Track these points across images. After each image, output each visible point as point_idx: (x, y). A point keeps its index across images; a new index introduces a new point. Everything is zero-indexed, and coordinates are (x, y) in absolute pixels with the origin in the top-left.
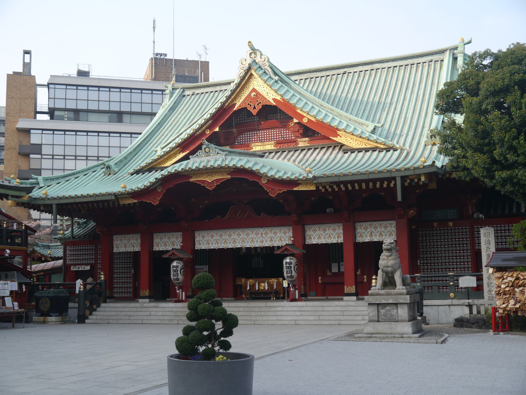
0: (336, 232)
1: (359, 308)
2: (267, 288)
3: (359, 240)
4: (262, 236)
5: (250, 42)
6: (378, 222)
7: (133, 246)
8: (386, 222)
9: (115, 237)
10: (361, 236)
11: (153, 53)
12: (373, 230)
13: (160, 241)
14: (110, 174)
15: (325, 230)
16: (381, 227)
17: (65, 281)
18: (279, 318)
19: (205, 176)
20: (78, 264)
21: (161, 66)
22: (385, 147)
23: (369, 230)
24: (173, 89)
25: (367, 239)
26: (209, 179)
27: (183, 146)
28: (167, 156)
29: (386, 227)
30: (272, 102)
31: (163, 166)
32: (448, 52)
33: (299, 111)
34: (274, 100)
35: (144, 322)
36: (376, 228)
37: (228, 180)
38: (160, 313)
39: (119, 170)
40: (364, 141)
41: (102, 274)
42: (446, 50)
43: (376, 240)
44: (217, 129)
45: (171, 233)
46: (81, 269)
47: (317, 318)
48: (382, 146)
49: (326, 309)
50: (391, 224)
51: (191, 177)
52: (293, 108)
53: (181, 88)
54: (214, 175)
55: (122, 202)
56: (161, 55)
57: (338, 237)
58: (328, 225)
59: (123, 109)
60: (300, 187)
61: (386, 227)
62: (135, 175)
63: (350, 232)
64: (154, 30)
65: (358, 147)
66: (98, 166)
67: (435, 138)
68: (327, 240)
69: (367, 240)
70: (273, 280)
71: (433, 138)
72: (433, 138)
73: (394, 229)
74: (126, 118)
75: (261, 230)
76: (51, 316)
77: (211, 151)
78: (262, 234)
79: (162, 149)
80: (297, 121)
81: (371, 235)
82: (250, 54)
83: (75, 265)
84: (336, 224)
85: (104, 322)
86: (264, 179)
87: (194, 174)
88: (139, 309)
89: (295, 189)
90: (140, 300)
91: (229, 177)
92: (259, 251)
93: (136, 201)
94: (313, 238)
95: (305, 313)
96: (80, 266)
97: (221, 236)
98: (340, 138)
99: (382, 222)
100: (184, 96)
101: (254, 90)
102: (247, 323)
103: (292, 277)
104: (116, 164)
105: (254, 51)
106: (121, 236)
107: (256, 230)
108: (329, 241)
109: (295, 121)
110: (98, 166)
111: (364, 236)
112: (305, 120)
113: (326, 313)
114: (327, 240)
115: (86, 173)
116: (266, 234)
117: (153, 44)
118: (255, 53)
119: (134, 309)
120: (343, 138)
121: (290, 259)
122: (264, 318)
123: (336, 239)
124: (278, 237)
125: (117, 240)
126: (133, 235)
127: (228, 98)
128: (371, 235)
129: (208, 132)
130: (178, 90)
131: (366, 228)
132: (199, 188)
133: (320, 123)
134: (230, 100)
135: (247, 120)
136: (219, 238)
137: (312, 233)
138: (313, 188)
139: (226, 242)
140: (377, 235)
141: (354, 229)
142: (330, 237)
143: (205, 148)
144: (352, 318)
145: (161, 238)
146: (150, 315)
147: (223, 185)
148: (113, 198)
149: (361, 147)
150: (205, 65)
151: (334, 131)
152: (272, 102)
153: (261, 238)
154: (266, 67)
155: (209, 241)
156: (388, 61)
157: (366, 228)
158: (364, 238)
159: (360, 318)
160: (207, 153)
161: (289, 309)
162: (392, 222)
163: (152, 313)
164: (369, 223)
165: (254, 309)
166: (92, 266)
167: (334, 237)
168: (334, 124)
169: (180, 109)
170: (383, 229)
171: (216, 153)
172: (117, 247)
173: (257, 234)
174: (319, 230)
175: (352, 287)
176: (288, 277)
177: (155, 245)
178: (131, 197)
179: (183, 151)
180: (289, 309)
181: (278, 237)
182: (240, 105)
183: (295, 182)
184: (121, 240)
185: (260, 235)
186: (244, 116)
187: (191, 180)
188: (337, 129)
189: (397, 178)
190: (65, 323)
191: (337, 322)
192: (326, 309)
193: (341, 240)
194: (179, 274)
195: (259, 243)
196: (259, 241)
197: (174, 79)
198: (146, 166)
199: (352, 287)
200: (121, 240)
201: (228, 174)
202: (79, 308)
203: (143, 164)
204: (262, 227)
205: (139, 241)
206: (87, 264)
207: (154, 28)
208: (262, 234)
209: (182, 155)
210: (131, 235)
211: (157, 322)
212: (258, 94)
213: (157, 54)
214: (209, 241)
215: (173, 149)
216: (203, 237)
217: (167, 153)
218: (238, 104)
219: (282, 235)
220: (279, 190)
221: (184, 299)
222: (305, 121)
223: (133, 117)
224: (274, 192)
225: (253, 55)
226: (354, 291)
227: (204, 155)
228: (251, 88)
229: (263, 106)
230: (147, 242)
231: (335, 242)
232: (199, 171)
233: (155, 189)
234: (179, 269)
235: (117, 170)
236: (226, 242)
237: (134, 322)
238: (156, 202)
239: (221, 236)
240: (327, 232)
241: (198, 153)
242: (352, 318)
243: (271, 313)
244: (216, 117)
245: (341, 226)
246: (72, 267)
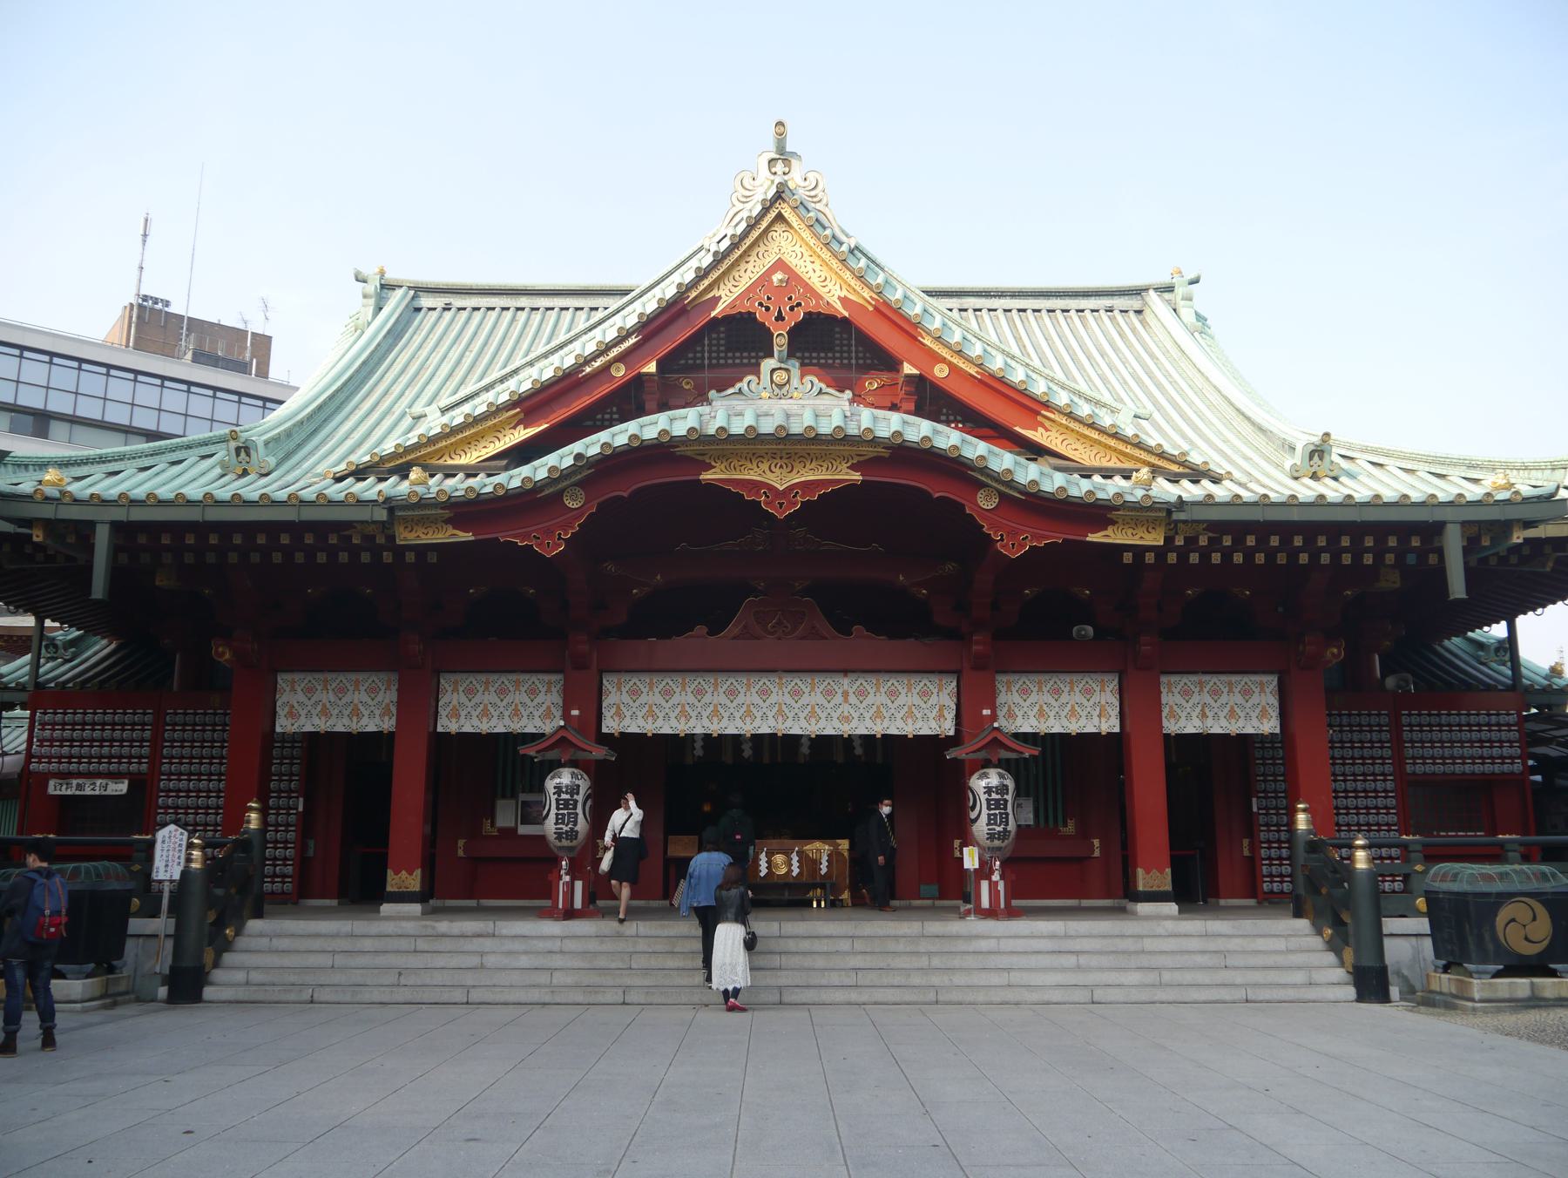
0: (1096, 698)
1: (1261, 944)
2: (796, 871)
3: (1171, 727)
4: (846, 700)
5: (780, 124)
6: (1224, 678)
7: (356, 713)
8: (1246, 679)
9: (283, 680)
10: (1173, 715)
11: (134, 291)
12: (1208, 699)
13: (463, 699)
14: (245, 473)
15: (1057, 692)
16: (1262, 691)
17: (20, 832)
18: (1016, 978)
19: (765, 466)
20: (79, 775)
21: (152, 323)
22: (1181, 470)
23: (1196, 698)
24: (383, 286)
25: (1191, 727)
26: (779, 478)
27: (529, 405)
28: (476, 428)
29: (1247, 693)
30: (838, 306)
31: (450, 462)
32: (1151, 292)
33: (927, 341)
34: (844, 300)
35: (476, 996)
36: (1215, 693)
37: (851, 487)
38: (524, 961)
39: (278, 465)
40: (1121, 446)
41: (251, 809)
42: (1147, 290)
43: (1216, 730)
44: (651, 368)
45: (514, 677)
46: (88, 791)
47: (1151, 977)
48: (1175, 468)
49: (1149, 944)
50: (1261, 684)
51: (709, 467)
52: (909, 329)
53: (410, 288)
54: (798, 466)
55: (406, 537)
56: (156, 301)
57: (1100, 716)
58: (1068, 677)
59: (52, 407)
60: (1109, 531)
61: (1247, 693)
62: (350, 480)
63: (1139, 704)
64: (144, 241)
65: (1096, 464)
66: (189, 447)
67: (1321, 459)
68: (1066, 723)
69: (1190, 730)
70: (817, 844)
71: (1316, 458)
72: (1316, 458)
73: (1274, 701)
74: (57, 428)
75: (846, 681)
76: (62, 976)
77: (795, 382)
78: (845, 694)
79: (444, 411)
80: (915, 372)
81: (1204, 715)
82: (772, 162)
83: (65, 776)
84: (1094, 676)
85: (292, 997)
86: (988, 497)
87: (722, 457)
88: (422, 945)
89: (1094, 538)
90: (386, 908)
91: (857, 477)
92: (747, 752)
93: (467, 537)
94: (1020, 714)
95: (1094, 961)
96: (88, 782)
97: (699, 692)
98: (1046, 434)
99: (1234, 678)
100: (418, 310)
101: (780, 265)
102: (907, 998)
103: (1004, 835)
104: (267, 443)
105: (783, 156)
106: (309, 677)
107: (824, 682)
108: (1074, 727)
109: (908, 369)
110: (189, 447)
111: (1183, 715)
112: (941, 370)
113: (1200, 959)
114: (1066, 723)
115: (147, 462)
116: (862, 694)
117: (137, 272)
118: (787, 162)
119: (404, 944)
120: (1053, 434)
121: (1001, 776)
122: (959, 979)
123: (1096, 720)
124: (912, 708)
125: (293, 690)
126: (361, 676)
127: (702, 274)
128: (1204, 715)
129: (620, 372)
130: (399, 293)
131: (1186, 693)
132: (735, 508)
133: (996, 385)
134: (706, 282)
135: (726, 358)
136: (691, 699)
137: (1016, 698)
138: (1155, 539)
139: (749, 713)
140: (1222, 715)
142: (1073, 712)
143: (773, 371)
144: (1273, 977)
145: (470, 692)
146: (482, 967)
147: (828, 508)
148: (381, 515)
149: (1111, 464)
150: (263, 343)
151: (1034, 407)
152: (838, 306)
153: (846, 708)
154: (818, 206)
156: (1001, 294)
157: (1186, 693)
158: (1182, 722)
159: (1299, 977)
160: (780, 386)
161: (1020, 945)
162: (1265, 678)
163: (491, 960)
164: (1194, 678)
165: (891, 946)
166: (137, 782)
167: (1089, 716)
168: (1039, 388)
169: (414, 338)
170: (1238, 698)
171: (816, 390)
172: (292, 714)
173: (829, 693)
174: (1040, 689)
175: (1161, 871)
176: (991, 837)
177: (443, 712)
178: (448, 521)
179: (526, 420)
180: (1020, 945)
181: (912, 708)
182: (732, 305)
183: (1099, 513)
184: (310, 691)
185: (839, 699)
186: (718, 345)
187: (706, 476)
188: (1047, 405)
189: (1449, 526)
190: (114, 1005)
191: (1240, 994)
192: (1149, 944)
193: (1110, 725)
194: (581, 816)
195: (836, 724)
196: (835, 715)
197: (189, 356)
198: (394, 456)
199: (1161, 871)
200: (310, 691)
201: (853, 468)
202: (178, 937)
203: (388, 447)
204: (845, 672)
205: (392, 696)
206: (115, 776)
207: (145, 235)
208: (845, 694)
209: (522, 434)
210: (353, 676)
211: (535, 995)
212: (793, 277)
213: (145, 298)
215: (495, 411)
216: (635, 693)
217: (478, 420)
218: (728, 297)
219: (917, 700)
220: (1034, 537)
221: (578, 904)
222: (940, 371)
223: (78, 429)
225: (779, 168)
226: (1168, 887)
227: (765, 394)
228: (770, 260)
229: (808, 315)
230: (418, 701)
231: (1090, 729)
232: (753, 445)
233: (559, 496)
234: (580, 798)
235: (272, 461)
236: (715, 713)
237: (428, 996)
238: (552, 548)
239: (699, 692)
240: (1064, 698)
241: (743, 385)
242: (1273, 977)
243: (970, 962)
244: (650, 328)
245: (1112, 682)
246: (52, 783)
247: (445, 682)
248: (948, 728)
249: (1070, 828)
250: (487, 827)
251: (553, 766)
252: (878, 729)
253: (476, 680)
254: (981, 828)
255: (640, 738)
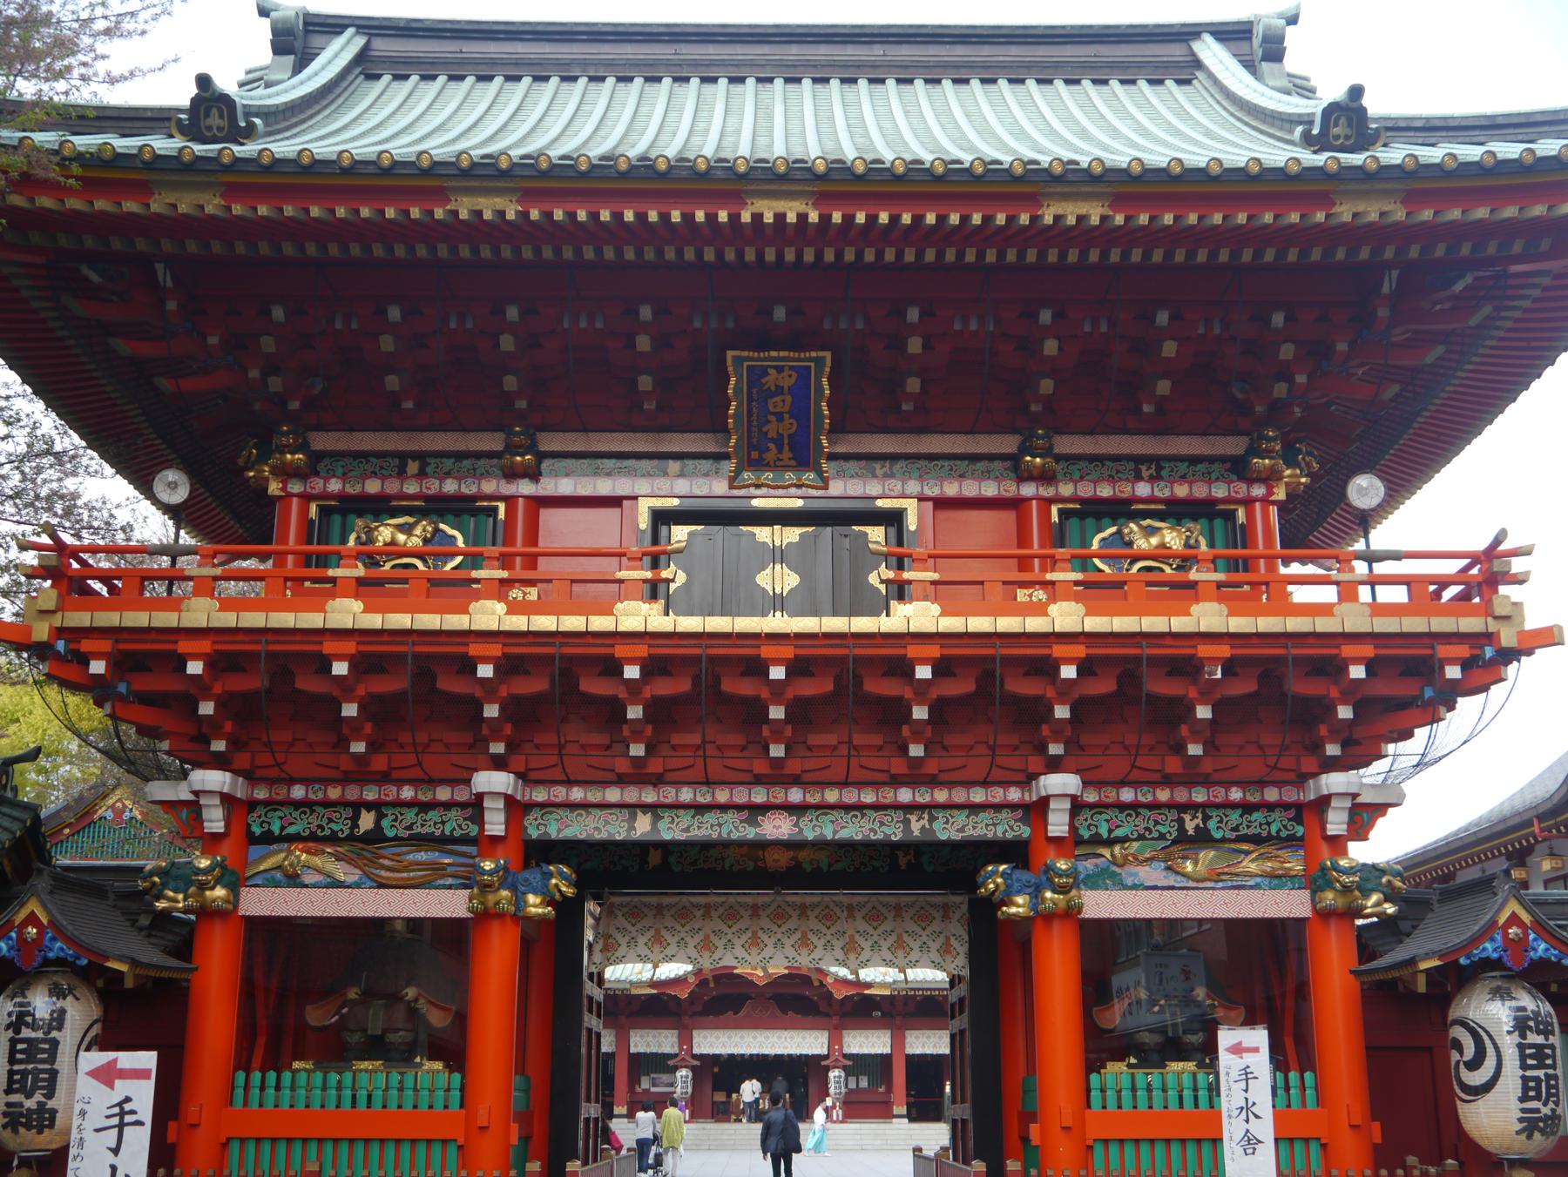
3: (909, 1051)
25: (918, 1051)
55: (635, 992)
63: (898, 1041)
108: (873, 1051)
138: (887, 993)
141: (904, 1038)
155: (715, 1042)
193: (887, 1050)
214: (715, 1042)
224: (839, 994)
238: (684, 994)
245: (888, 1033)
247: (632, 1033)
248: (826, 1052)
249: (882, 1090)
250: (638, 1090)
251: (675, 1069)
252: (798, 1052)
253: (643, 1032)
254: (832, 1091)
255: (708, 1055)
